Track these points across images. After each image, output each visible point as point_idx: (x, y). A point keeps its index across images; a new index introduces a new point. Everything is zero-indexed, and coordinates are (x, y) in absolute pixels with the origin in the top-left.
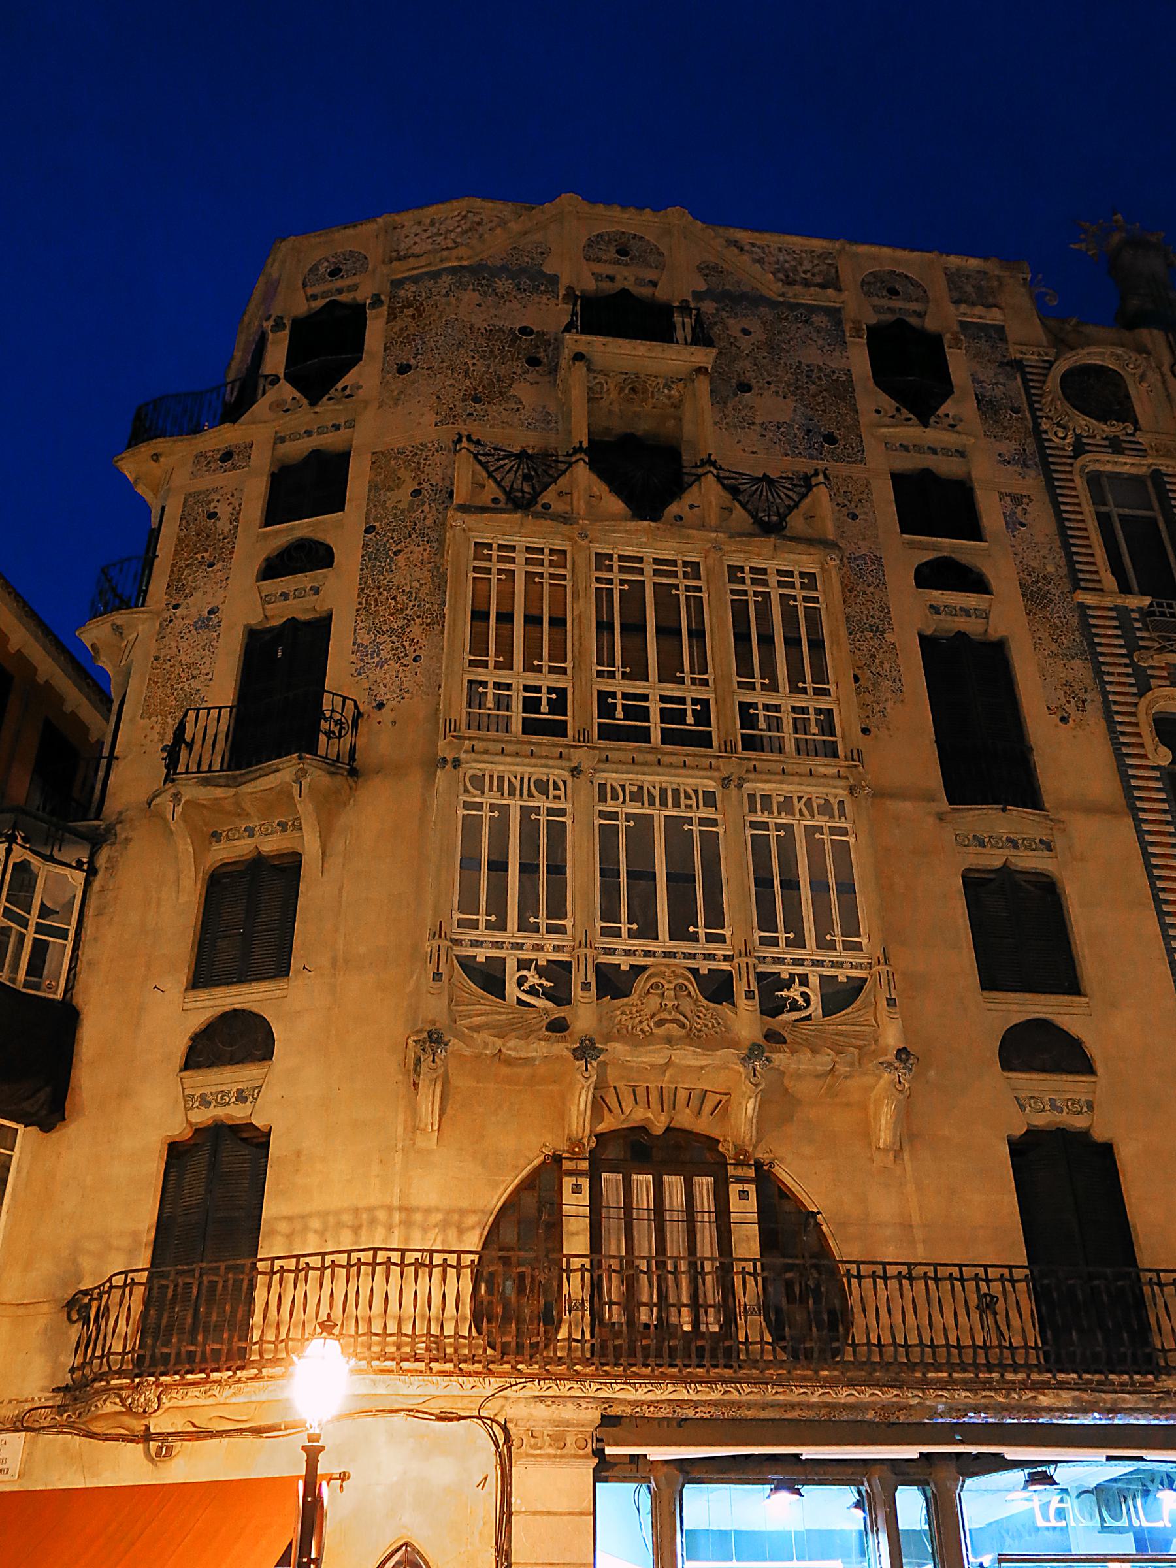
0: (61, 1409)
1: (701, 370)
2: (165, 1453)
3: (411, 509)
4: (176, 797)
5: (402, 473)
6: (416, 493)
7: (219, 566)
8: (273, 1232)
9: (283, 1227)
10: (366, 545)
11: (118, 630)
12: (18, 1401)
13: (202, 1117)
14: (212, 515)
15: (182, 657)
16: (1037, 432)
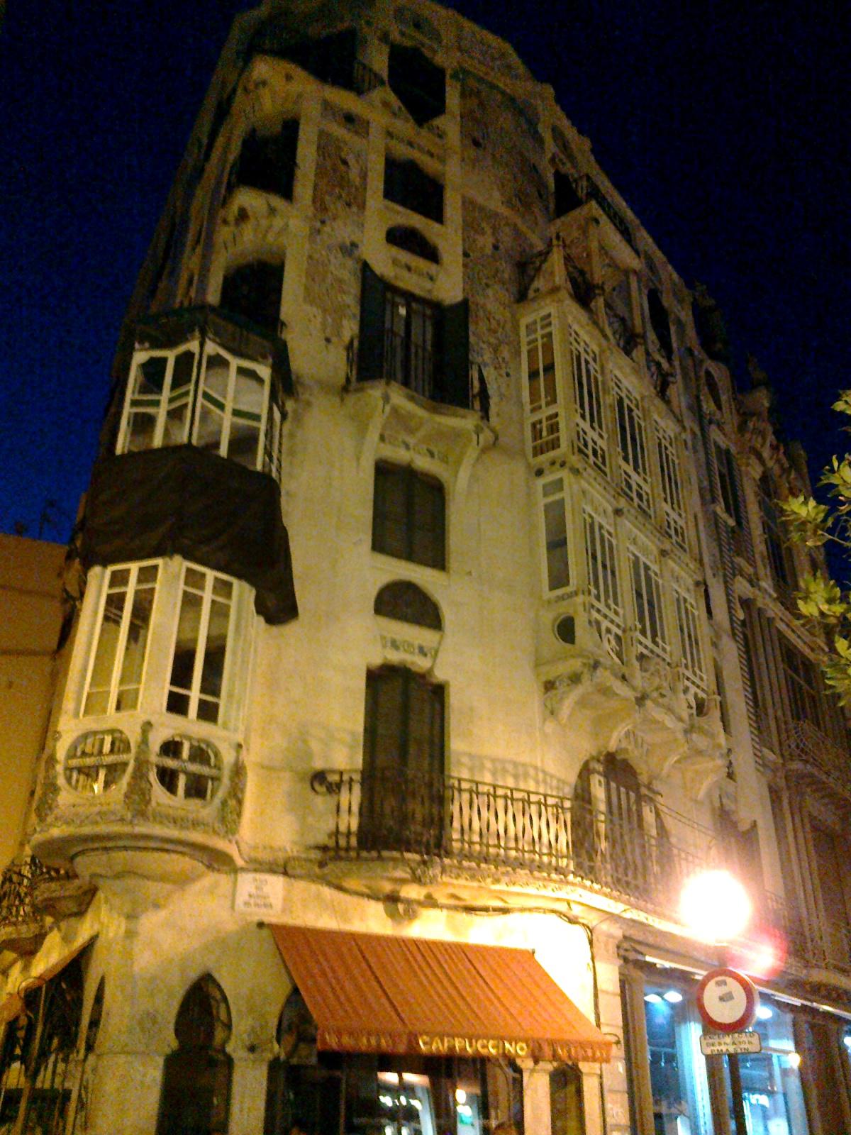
0: (322, 864)
1: (635, 272)
2: (410, 915)
3: (493, 256)
4: (386, 399)
5: (484, 225)
6: (496, 247)
7: (354, 209)
8: (459, 763)
9: (465, 760)
10: (465, 266)
11: (272, 211)
12: (271, 848)
13: (395, 657)
14: (345, 162)
15: (332, 268)
16: (697, 397)
